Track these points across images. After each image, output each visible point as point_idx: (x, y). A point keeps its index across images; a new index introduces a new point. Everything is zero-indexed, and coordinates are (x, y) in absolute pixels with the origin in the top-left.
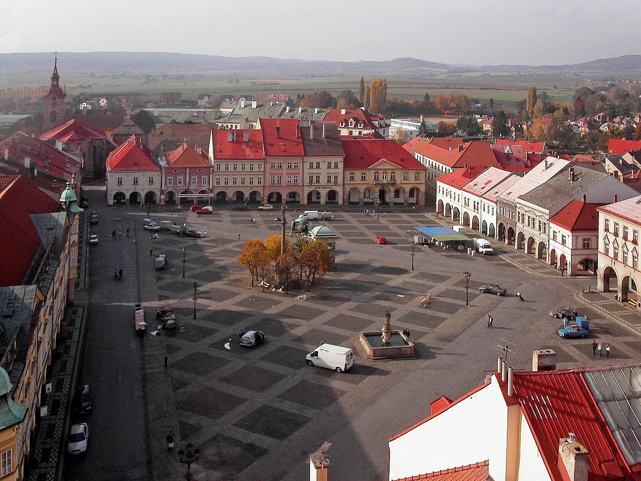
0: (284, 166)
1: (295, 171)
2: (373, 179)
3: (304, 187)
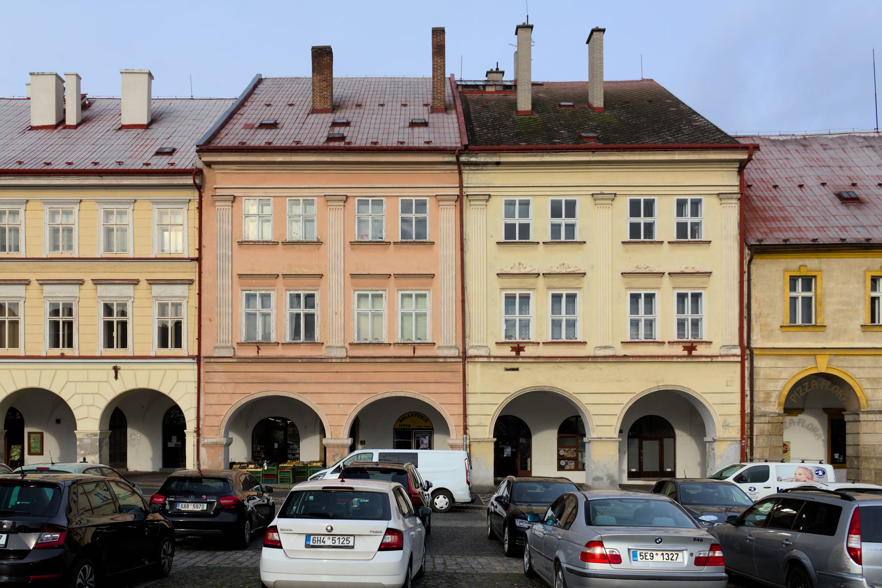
3: (470, 368)
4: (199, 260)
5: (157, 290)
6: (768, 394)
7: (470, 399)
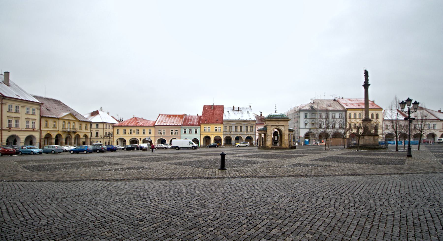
0: (23, 111)
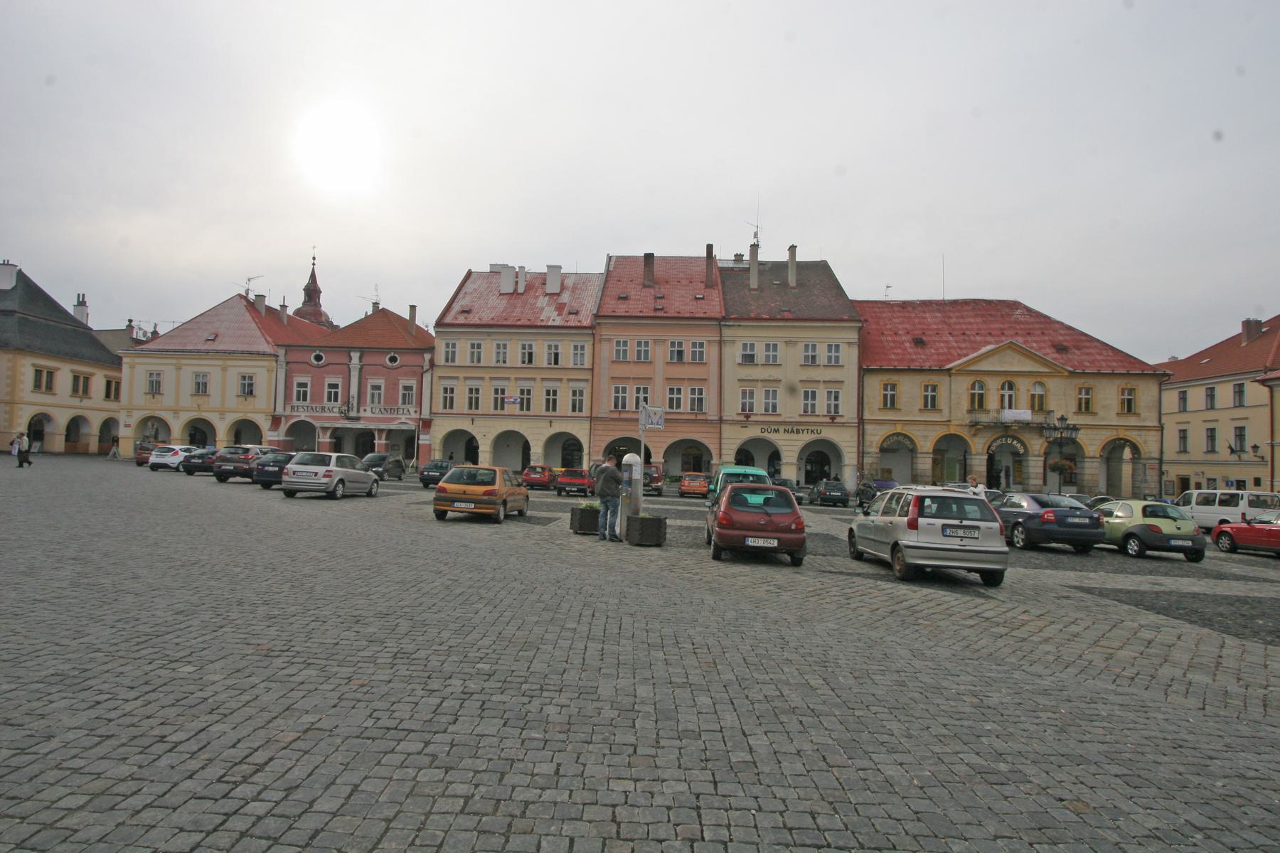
1: (697, 372)
2: (965, 404)
3: (725, 427)
4: (592, 370)
5: (572, 384)
6: (872, 442)
7: (723, 441)
